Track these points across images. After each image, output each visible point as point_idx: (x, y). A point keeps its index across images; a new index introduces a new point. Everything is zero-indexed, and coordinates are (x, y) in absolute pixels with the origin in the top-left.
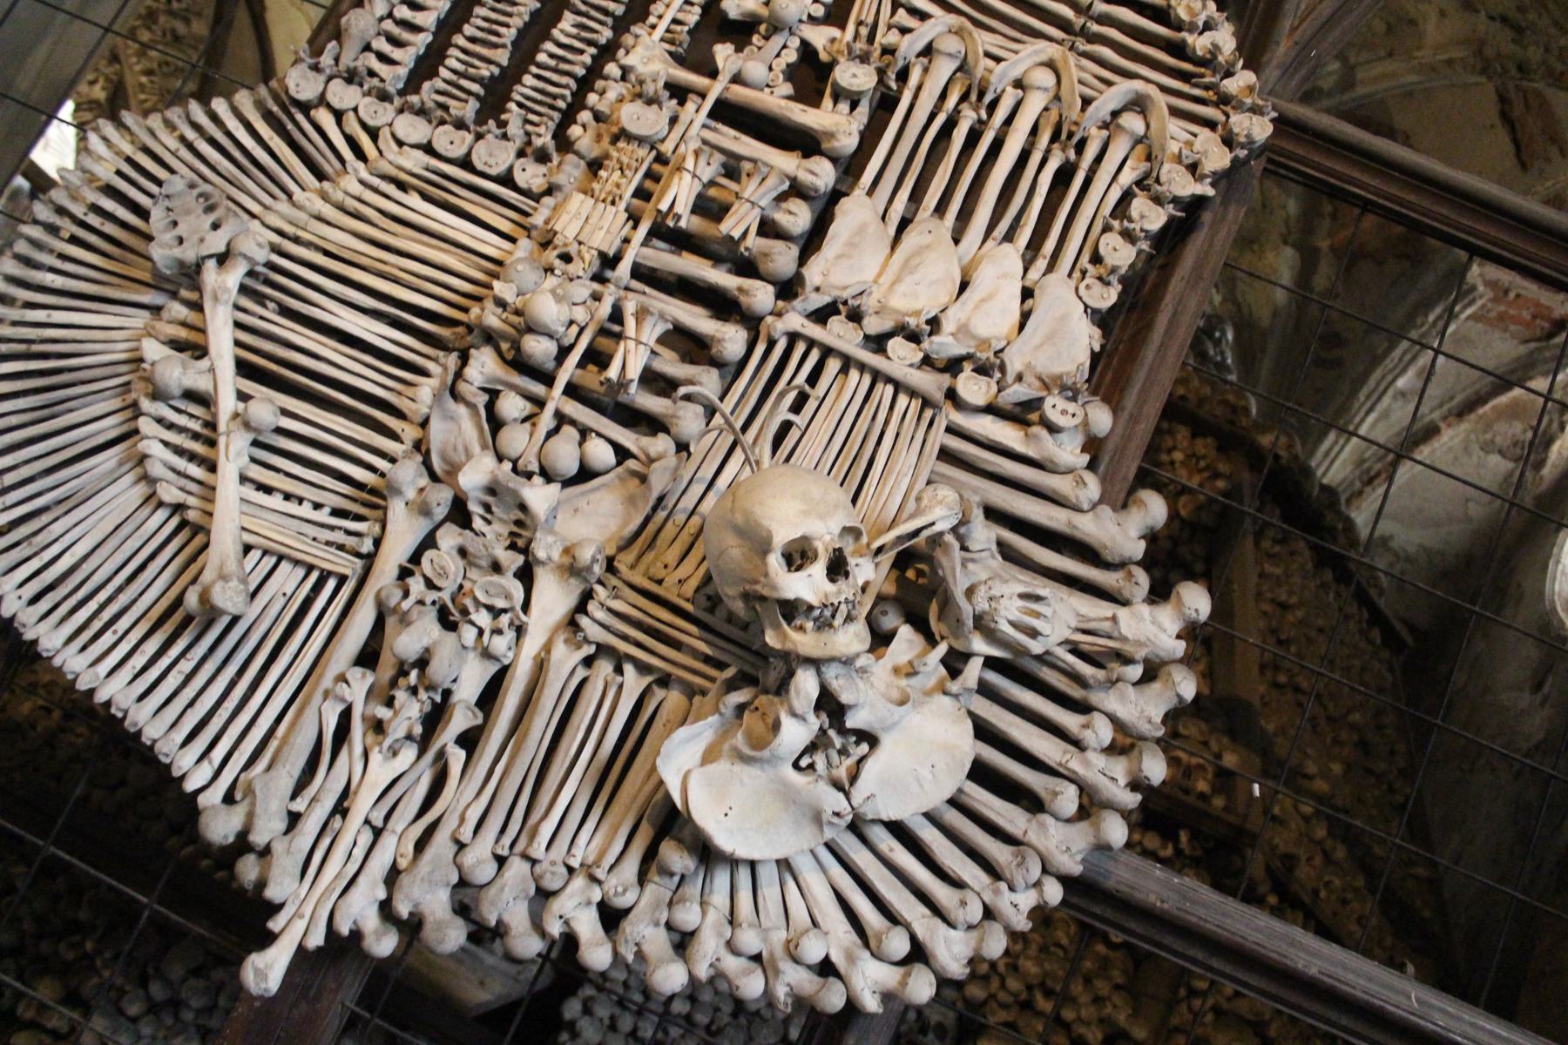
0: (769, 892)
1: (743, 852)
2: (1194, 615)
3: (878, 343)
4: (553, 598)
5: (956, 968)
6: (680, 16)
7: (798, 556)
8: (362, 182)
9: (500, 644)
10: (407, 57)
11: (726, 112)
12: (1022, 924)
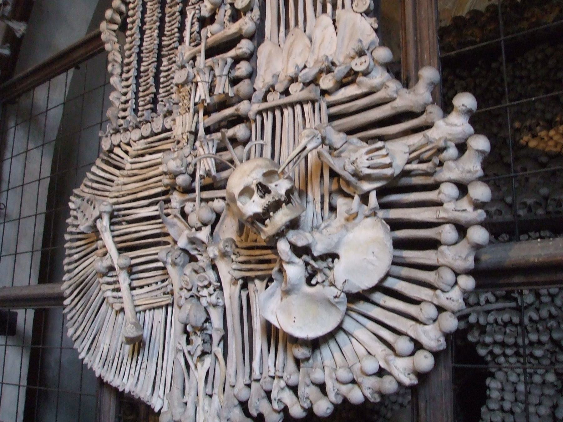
0: (347, 349)
2: (464, 108)
6: (192, 30)
8: (132, 163)
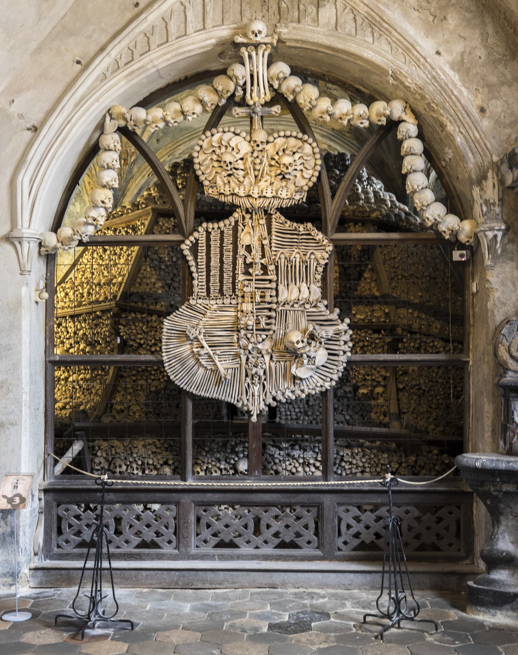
0: (310, 380)
1: (305, 377)
3: (293, 306)
4: (267, 358)
5: (337, 379)
7: (298, 342)
9: (264, 366)
10: (205, 290)
11: (256, 280)
12: (343, 370)
